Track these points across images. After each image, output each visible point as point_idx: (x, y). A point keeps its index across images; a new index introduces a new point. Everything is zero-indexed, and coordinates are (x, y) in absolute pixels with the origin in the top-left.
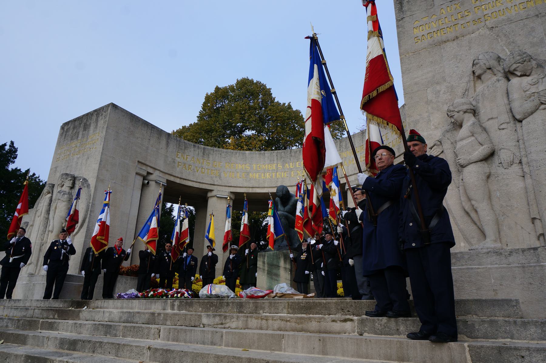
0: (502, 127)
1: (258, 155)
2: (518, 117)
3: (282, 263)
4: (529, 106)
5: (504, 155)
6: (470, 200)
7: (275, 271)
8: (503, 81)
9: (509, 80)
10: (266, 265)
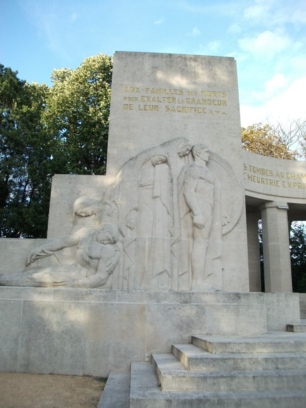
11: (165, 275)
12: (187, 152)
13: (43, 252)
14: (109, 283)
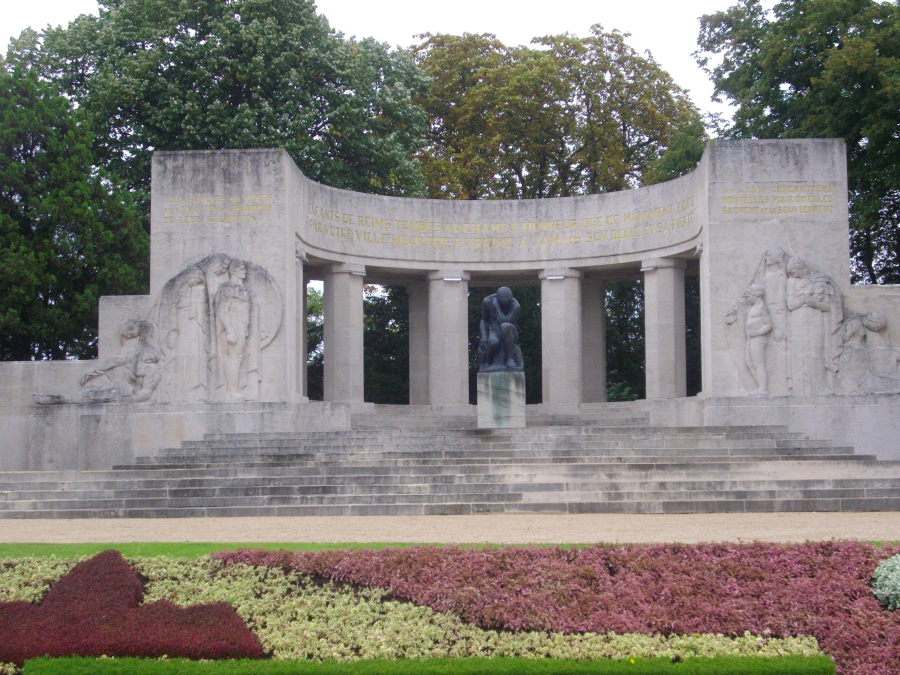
0: (779, 312)
1: (402, 205)
2: (790, 308)
3: (513, 387)
4: (797, 302)
5: (777, 333)
6: (752, 360)
7: (503, 396)
8: (784, 276)
9: (788, 277)
10: (490, 389)
11: (201, 388)
12: (224, 271)
13: (95, 372)
14: (153, 397)
